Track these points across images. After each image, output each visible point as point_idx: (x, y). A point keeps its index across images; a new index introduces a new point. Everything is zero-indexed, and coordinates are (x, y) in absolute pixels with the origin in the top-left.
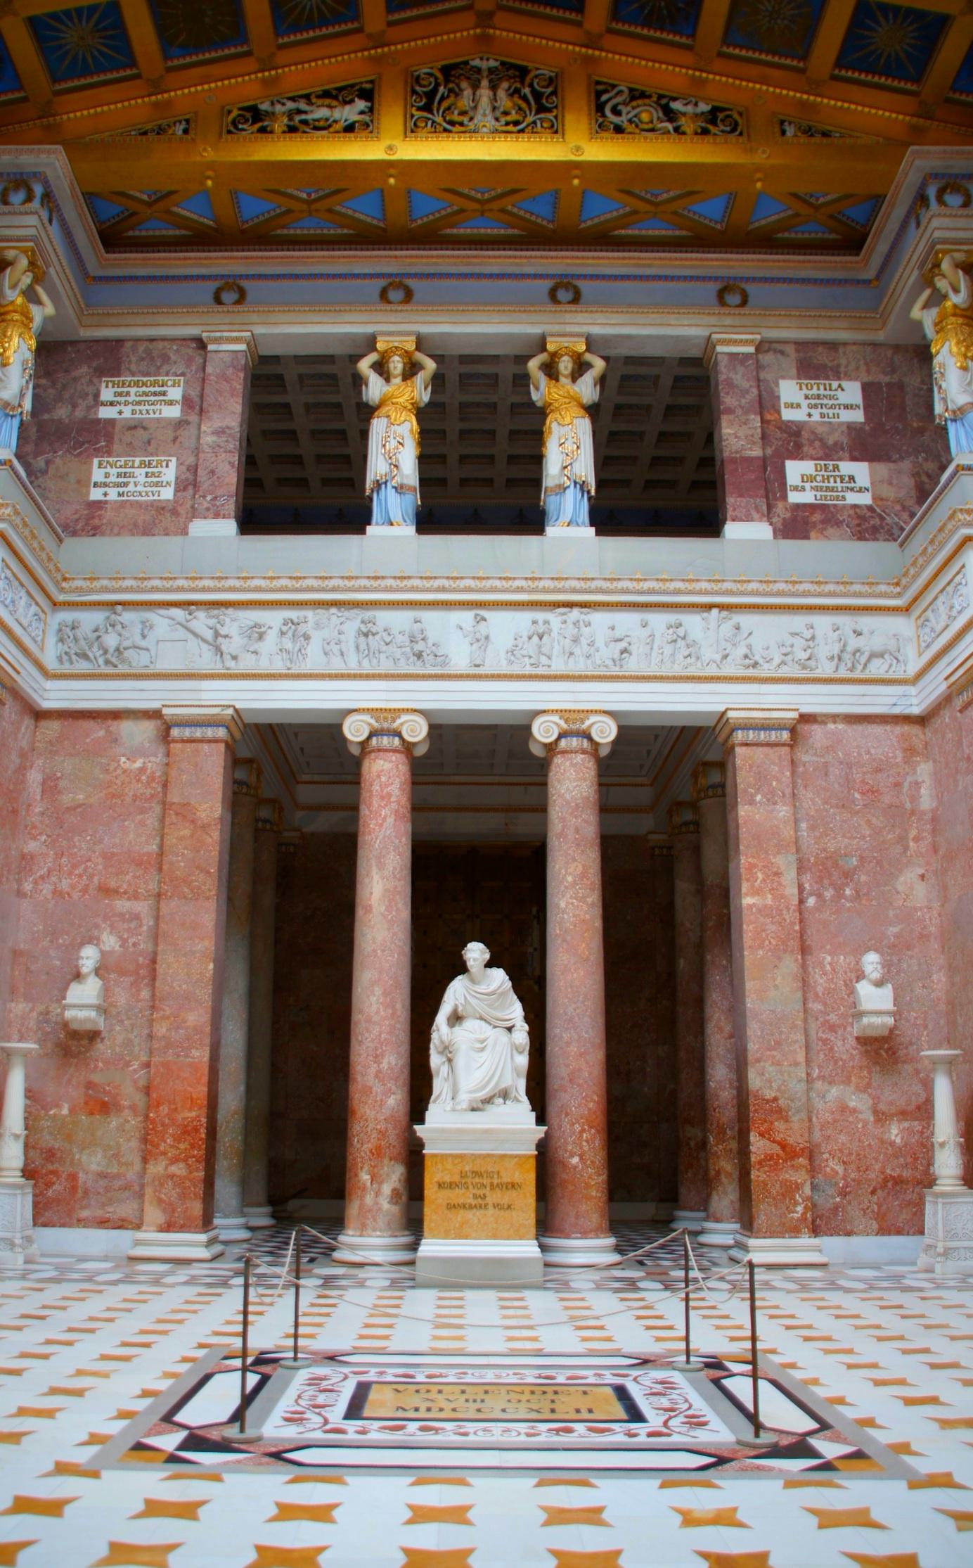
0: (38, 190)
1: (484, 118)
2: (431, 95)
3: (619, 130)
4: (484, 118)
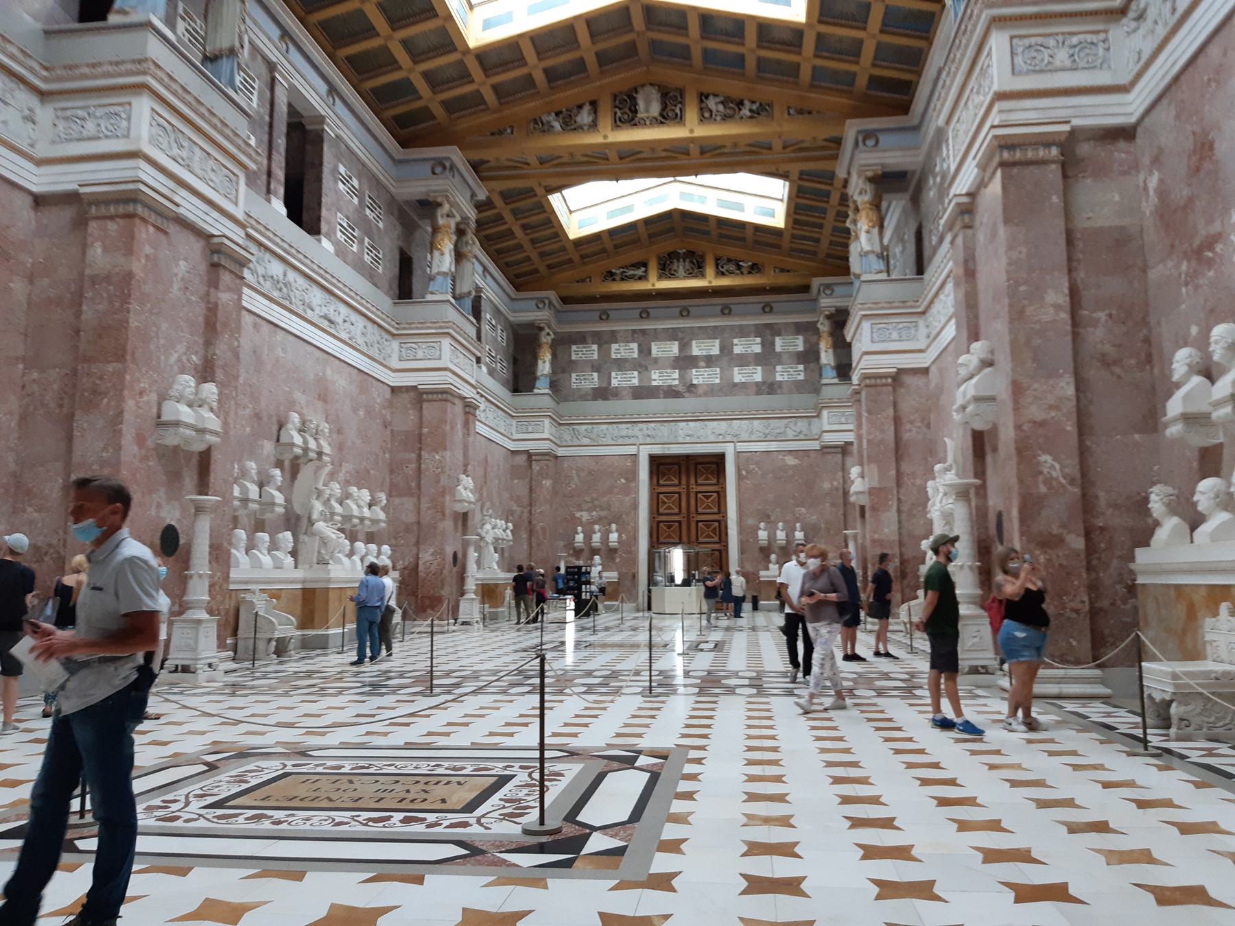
0: (547, 302)
1: (681, 271)
2: (664, 265)
3: (723, 274)
4: (681, 271)
